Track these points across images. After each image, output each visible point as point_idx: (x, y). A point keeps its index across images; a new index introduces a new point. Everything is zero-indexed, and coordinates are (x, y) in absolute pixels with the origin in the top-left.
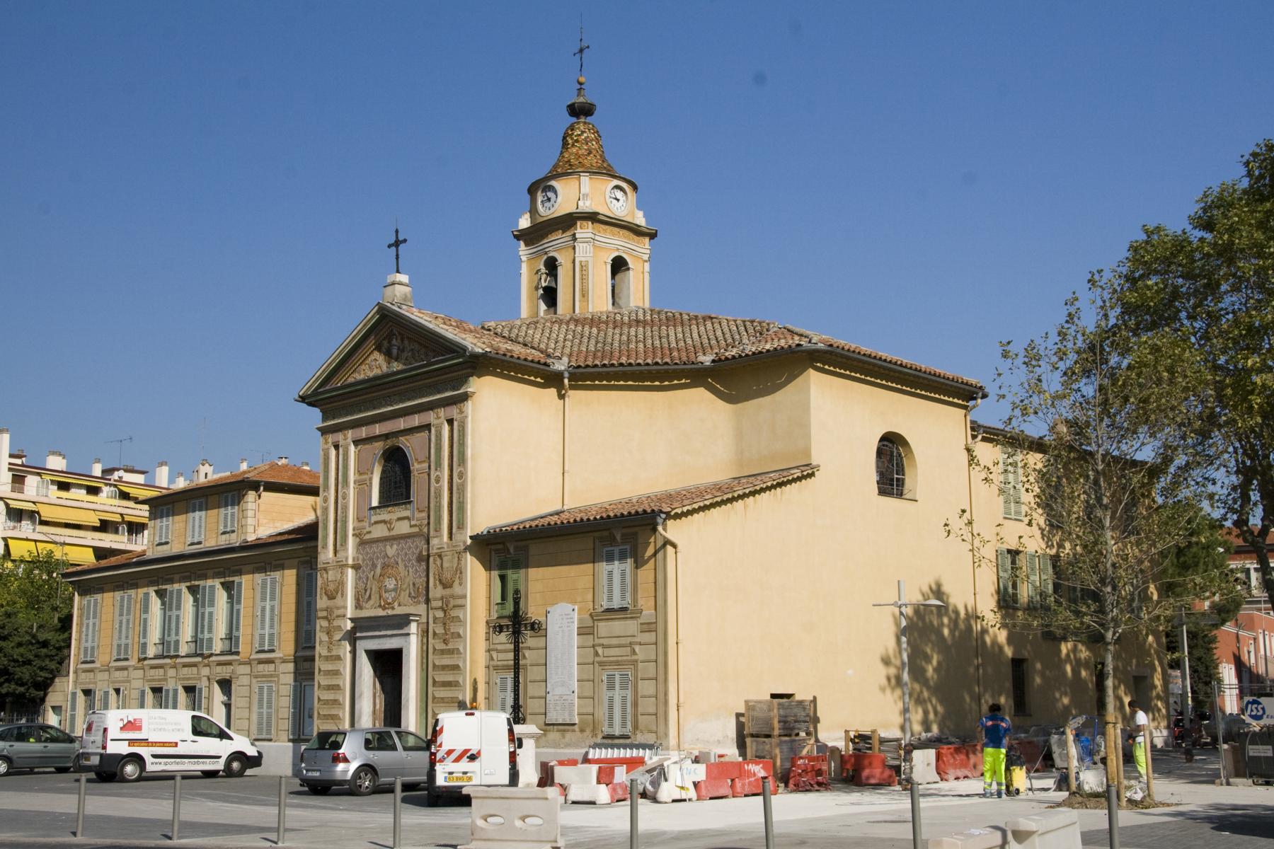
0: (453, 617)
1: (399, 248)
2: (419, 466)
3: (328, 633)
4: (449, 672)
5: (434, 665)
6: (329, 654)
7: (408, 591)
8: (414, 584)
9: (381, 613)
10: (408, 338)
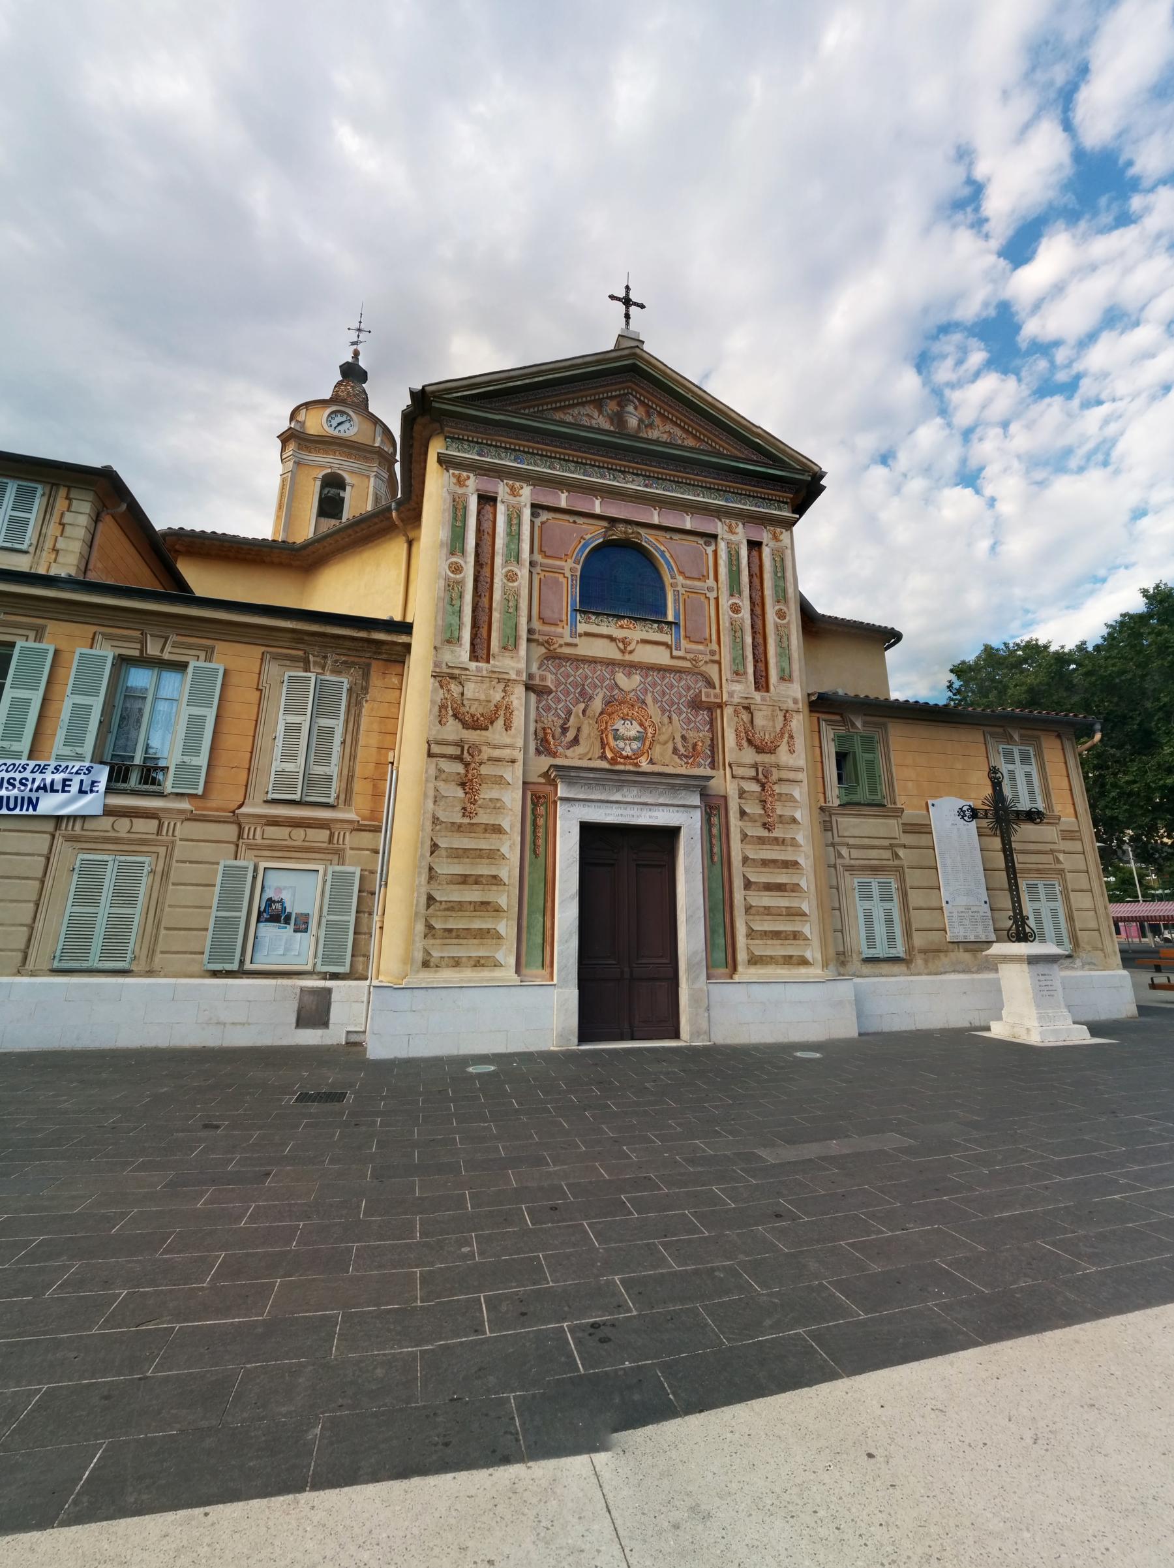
0: (780, 794)
2: (688, 582)
3: (463, 784)
5: (745, 860)
6: (466, 820)
7: (670, 746)
8: (684, 738)
9: (605, 765)
10: (659, 413)
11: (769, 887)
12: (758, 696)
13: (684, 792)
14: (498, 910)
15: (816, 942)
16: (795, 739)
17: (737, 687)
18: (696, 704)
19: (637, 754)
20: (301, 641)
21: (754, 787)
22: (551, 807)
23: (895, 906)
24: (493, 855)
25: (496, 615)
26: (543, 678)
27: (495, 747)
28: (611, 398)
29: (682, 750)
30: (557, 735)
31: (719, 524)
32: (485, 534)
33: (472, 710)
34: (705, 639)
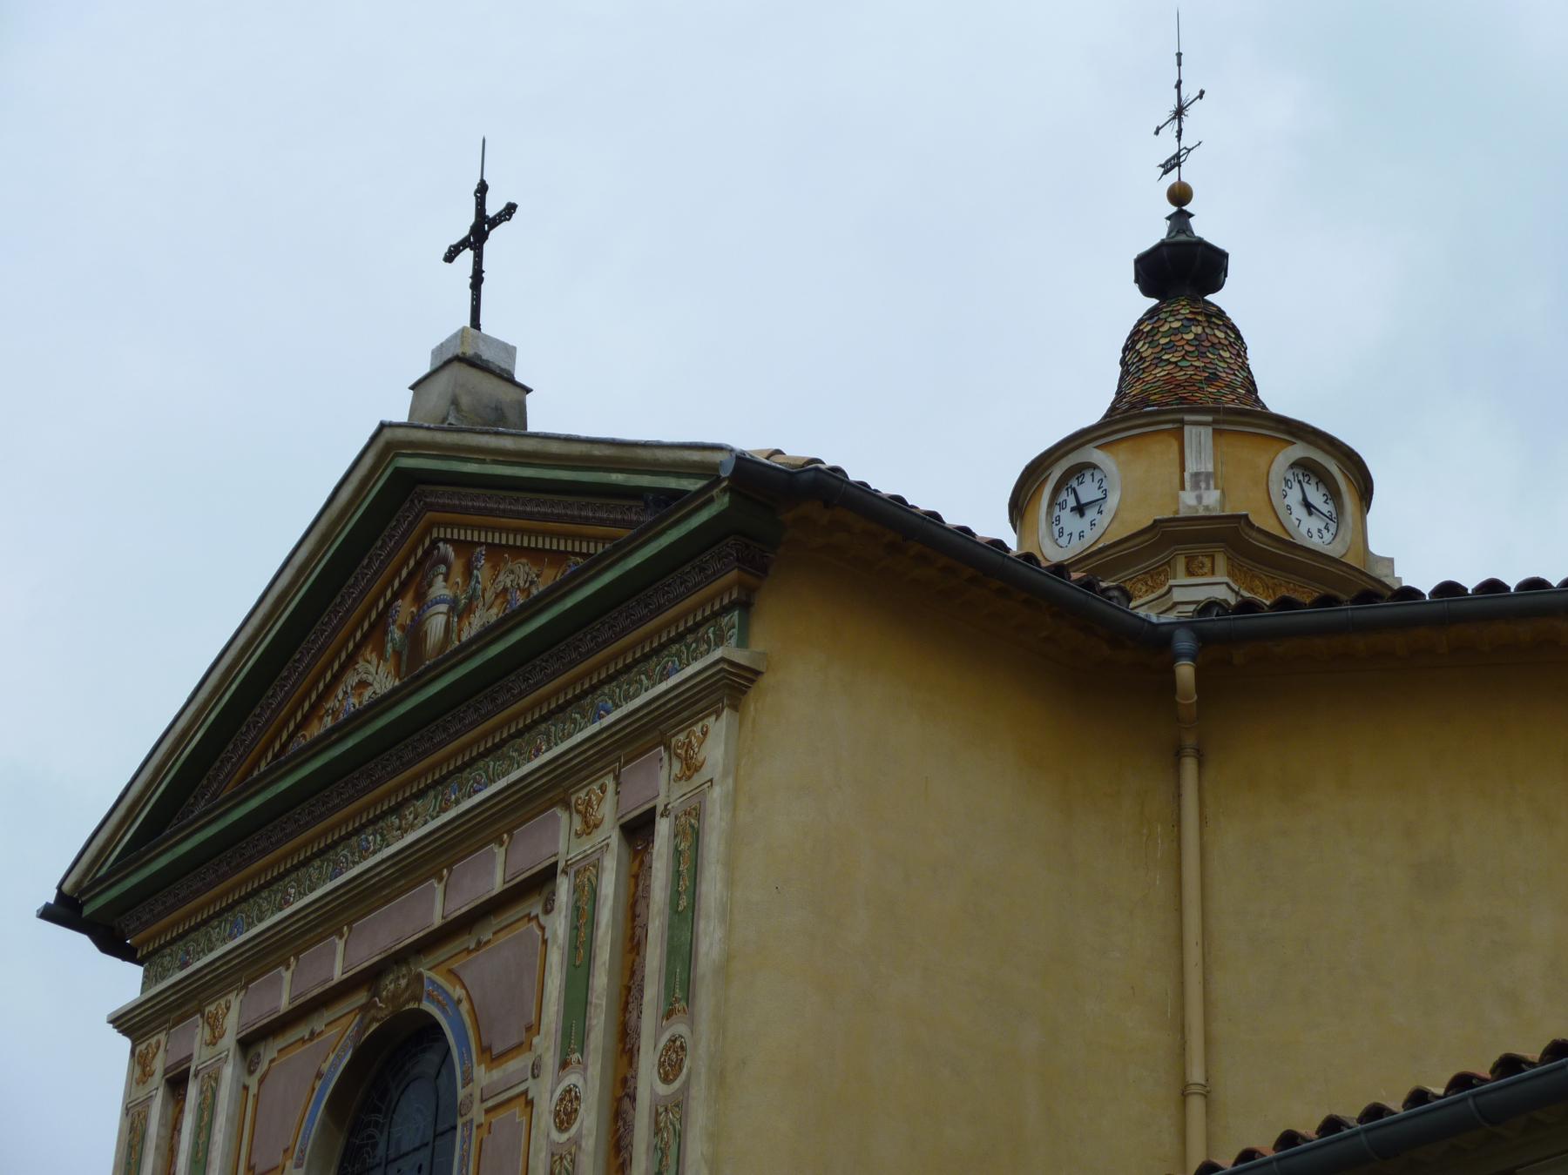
2: (497, 1074)
31: (563, 815)
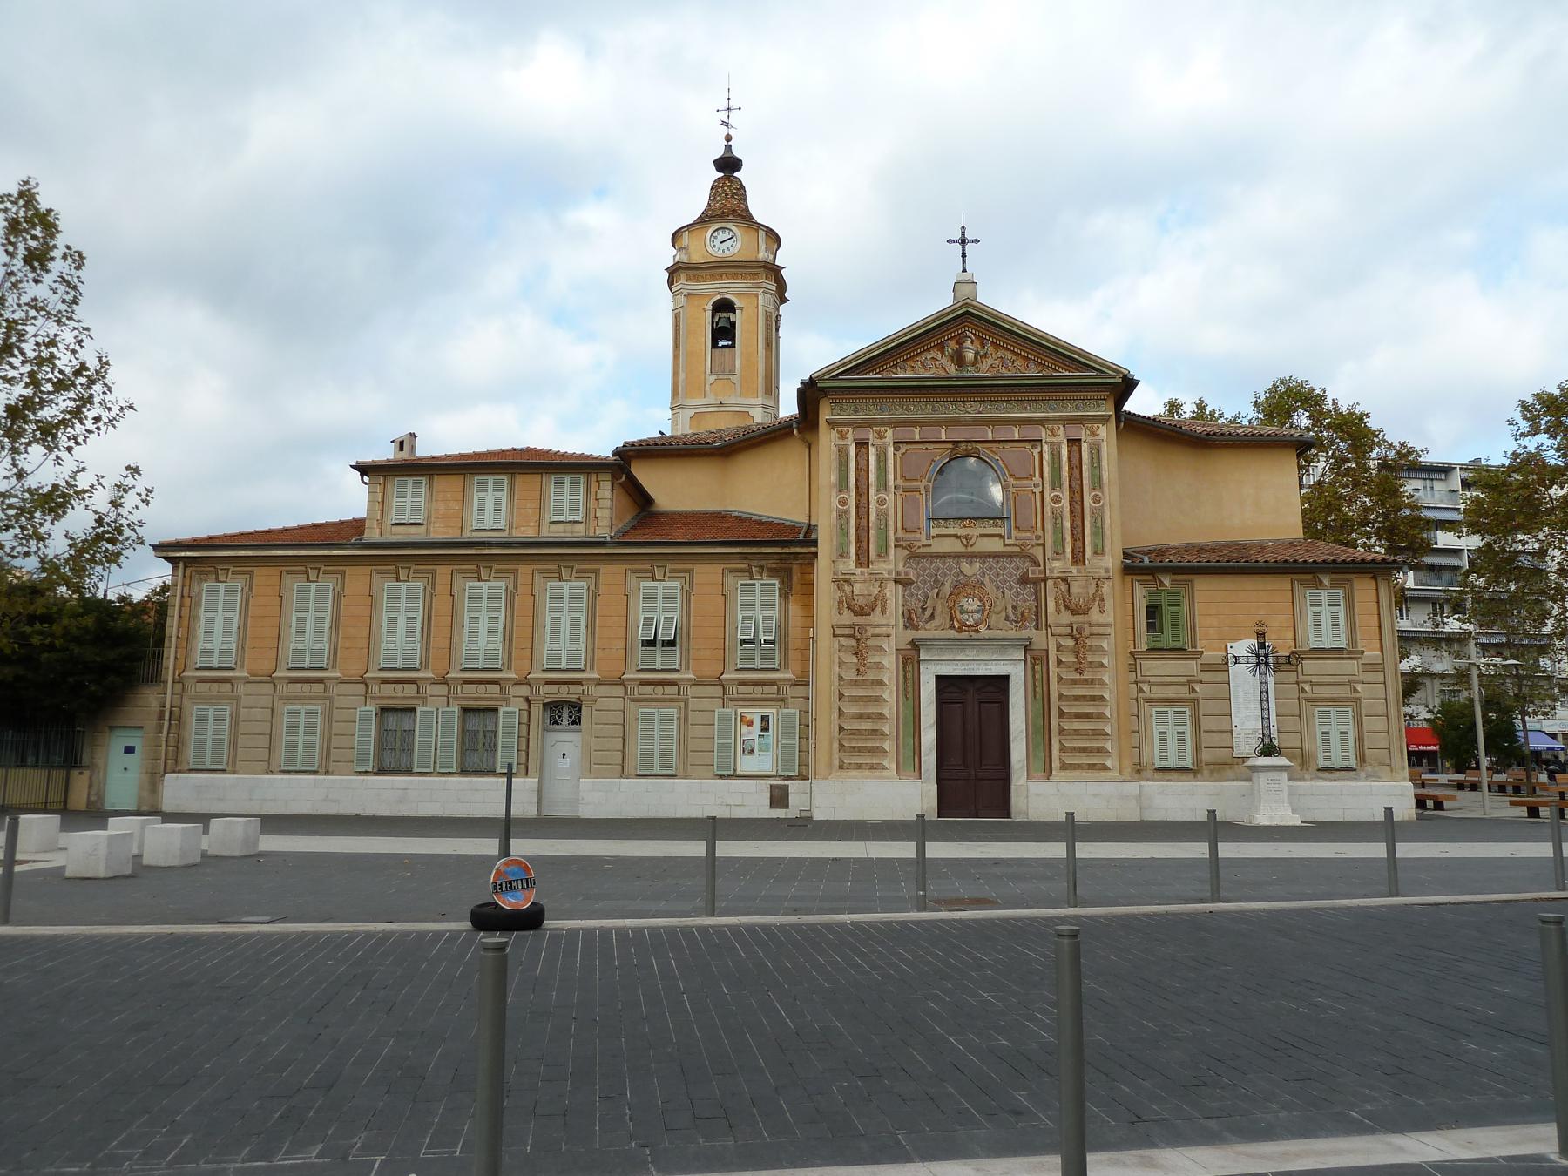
1: (966, 247)
2: (1018, 482)
3: (856, 654)
4: (1086, 703)
5: (1060, 696)
7: (1003, 615)
8: (1014, 608)
9: (953, 634)
11: (1078, 716)
12: (1074, 570)
13: (1012, 650)
14: (883, 734)
15: (1115, 754)
16: (1106, 601)
17: (1057, 564)
18: (1024, 580)
19: (978, 623)
20: (746, 559)
21: (1071, 642)
22: (916, 665)
23: (1188, 730)
24: (877, 700)
25: (872, 532)
26: (907, 573)
27: (876, 626)
28: (952, 338)
29: (1013, 617)
30: (918, 614)
32: (862, 471)
33: (859, 603)
34: (1032, 527)
